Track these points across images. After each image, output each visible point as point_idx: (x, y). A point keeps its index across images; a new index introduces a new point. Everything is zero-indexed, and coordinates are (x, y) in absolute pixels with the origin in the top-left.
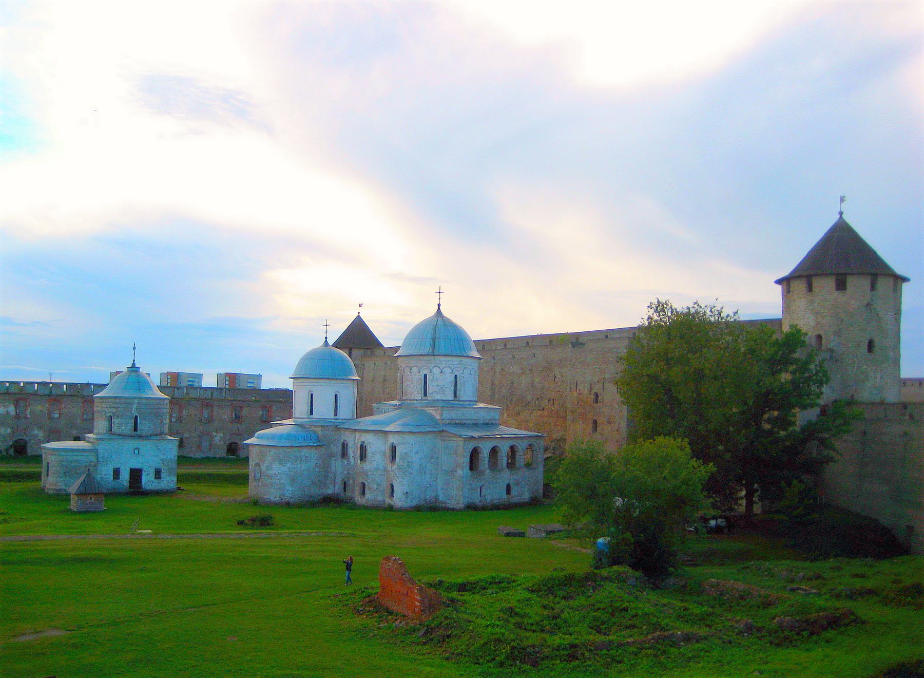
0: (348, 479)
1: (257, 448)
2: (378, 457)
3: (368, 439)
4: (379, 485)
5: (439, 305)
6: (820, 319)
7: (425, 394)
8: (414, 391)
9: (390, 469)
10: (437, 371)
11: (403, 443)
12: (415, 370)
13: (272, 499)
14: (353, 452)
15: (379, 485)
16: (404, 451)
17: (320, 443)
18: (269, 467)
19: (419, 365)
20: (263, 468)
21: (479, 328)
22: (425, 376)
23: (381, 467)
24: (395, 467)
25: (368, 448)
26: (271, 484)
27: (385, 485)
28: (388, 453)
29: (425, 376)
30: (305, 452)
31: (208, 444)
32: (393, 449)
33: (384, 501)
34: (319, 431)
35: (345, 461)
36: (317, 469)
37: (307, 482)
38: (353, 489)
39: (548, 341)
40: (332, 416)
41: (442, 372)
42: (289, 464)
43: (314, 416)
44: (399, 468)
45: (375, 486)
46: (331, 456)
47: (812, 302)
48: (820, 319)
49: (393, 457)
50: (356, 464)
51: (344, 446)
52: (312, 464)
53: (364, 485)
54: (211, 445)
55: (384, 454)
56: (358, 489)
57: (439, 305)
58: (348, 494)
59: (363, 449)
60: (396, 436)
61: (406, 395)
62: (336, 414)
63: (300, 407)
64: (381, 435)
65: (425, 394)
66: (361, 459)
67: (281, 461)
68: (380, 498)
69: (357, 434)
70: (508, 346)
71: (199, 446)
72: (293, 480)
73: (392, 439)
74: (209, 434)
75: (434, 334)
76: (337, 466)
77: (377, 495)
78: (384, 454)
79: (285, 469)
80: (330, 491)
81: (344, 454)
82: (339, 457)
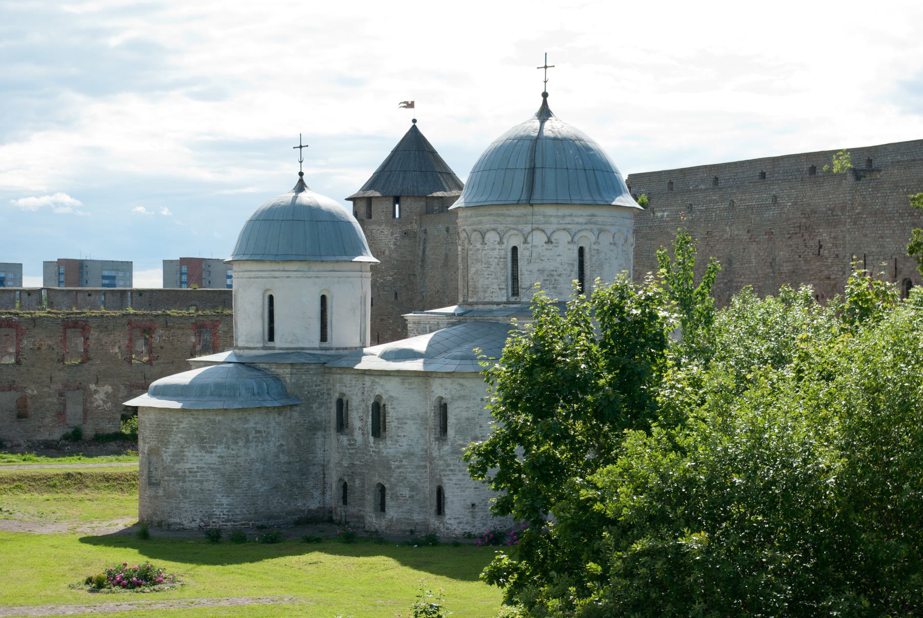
0: (352, 476)
1: (152, 416)
3: (389, 389)
4: (413, 488)
5: (545, 95)
7: (515, 293)
8: (490, 285)
9: (435, 454)
10: (539, 239)
11: (463, 397)
12: (492, 237)
13: (186, 524)
14: (359, 419)
15: (413, 488)
16: (465, 415)
17: (289, 400)
18: (179, 457)
19: (501, 228)
20: (167, 457)
21: (635, 146)
22: (515, 249)
23: (417, 450)
24: (447, 448)
25: (389, 408)
26: (183, 492)
27: (428, 489)
28: (433, 421)
29: (515, 249)
30: (255, 421)
31: (79, 409)
32: (443, 409)
33: (426, 524)
34: (285, 372)
35: (344, 439)
36: (283, 458)
37: (260, 486)
38: (363, 499)
39: (806, 167)
40: (313, 340)
41: (549, 241)
42: (220, 450)
43: (279, 342)
45: (406, 492)
46: (315, 427)
50: (366, 443)
51: (342, 405)
52: (272, 447)
53: (382, 489)
54: (85, 412)
55: (424, 420)
56: (371, 497)
57: (545, 95)
58: (352, 509)
59: (378, 411)
60: (448, 382)
61: (475, 292)
62: (324, 338)
63: (247, 323)
64: (416, 380)
65: (515, 293)
67: (203, 443)
68: (417, 517)
69: (367, 378)
70: (722, 183)
71: (61, 415)
72: (230, 482)
74: (81, 387)
75: (533, 159)
76: (332, 451)
77: (410, 511)
79: (211, 459)
80: (314, 505)
81: (342, 424)
82: (333, 431)
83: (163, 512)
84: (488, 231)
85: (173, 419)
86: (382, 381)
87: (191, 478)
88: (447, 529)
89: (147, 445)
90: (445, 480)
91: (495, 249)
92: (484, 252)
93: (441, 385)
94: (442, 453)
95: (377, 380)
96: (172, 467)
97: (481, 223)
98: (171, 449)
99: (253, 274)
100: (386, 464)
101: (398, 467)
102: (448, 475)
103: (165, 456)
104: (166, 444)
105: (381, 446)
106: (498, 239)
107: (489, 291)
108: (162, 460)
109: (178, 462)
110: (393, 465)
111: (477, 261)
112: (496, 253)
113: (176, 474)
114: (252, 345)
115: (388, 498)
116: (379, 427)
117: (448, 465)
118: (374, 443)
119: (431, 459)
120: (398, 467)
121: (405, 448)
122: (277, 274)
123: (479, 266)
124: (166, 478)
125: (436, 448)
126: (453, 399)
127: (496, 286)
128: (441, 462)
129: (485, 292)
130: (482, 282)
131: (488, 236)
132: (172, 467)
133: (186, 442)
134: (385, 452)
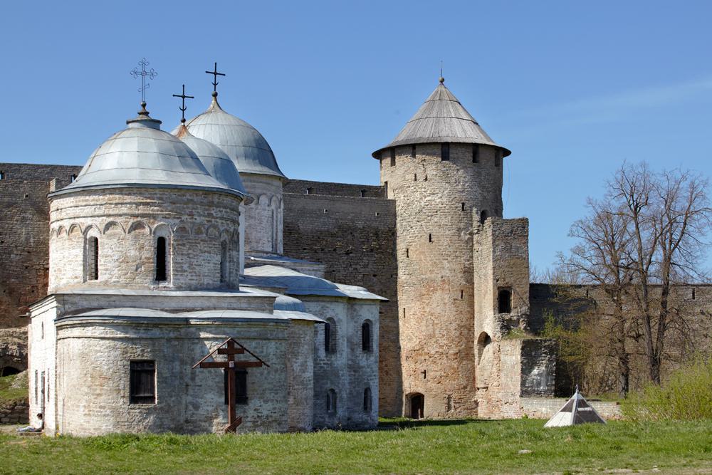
5: (215, 95)
6: (486, 194)
24: (372, 359)
28: (358, 339)
32: (366, 327)
48: (486, 194)
49: (366, 346)
66: (327, 349)
78: (349, 341)
83: (293, 418)
84: (260, 195)
85: (301, 332)
88: (373, 420)
91: (265, 210)
92: (258, 211)
93: (368, 310)
95: (328, 305)
96: (300, 376)
98: (301, 360)
102: (373, 379)
105: (333, 359)
108: (293, 370)
109: (304, 372)
118: (326, 356)
119: (354, 368)
120: (342, 376)
124: (296, 387)
125: (364, 359)
127: (266, 239)
128: (369, 370)
129: (258, 242)
131: (261, 198)
132: (300, 376)
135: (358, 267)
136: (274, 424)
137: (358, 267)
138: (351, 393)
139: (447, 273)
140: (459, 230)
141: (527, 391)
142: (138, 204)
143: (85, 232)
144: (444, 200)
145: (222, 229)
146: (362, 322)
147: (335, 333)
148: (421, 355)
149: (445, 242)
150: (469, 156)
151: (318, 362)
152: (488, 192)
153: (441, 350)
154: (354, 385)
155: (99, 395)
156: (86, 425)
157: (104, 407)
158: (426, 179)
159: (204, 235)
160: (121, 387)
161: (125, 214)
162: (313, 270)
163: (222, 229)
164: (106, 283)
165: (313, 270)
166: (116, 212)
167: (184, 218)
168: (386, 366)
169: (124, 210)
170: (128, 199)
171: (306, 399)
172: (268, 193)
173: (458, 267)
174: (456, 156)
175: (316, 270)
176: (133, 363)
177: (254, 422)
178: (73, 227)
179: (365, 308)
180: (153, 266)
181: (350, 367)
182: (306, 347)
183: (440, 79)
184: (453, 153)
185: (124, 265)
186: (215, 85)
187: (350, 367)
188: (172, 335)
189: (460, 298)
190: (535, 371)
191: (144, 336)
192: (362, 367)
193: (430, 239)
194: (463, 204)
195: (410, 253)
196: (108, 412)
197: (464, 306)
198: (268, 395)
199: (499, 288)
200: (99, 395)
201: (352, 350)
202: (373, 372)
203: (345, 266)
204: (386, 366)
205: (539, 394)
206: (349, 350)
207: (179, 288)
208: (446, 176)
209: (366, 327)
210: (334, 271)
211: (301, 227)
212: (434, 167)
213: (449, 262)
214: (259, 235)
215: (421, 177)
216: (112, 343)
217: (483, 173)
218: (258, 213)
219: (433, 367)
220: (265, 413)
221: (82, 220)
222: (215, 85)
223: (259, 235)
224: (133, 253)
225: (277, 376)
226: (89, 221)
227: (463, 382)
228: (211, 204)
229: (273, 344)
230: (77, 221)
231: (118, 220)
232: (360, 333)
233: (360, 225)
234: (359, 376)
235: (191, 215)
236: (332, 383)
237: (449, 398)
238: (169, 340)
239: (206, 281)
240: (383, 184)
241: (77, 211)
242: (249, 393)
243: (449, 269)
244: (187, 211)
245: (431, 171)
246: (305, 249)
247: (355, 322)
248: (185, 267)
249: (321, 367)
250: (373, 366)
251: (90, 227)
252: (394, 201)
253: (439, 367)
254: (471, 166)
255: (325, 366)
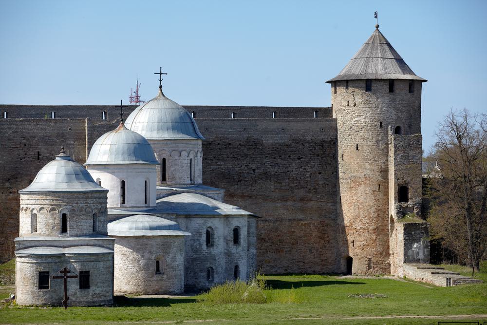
1: (158, 240)
2: (222, 240)
3: (216, 223)
5: (161, 87)
6: (399, 114)
12: (184, 154)
18: (174, 259)
22: (191, 160)
24: (240, 248)
28: (231, 237)
29: (191, 160)
32: (236, 232)
44: (243, 250)
47: (394, 100)
48: (399, 114)
56: (205, 274)
57: (161, 87)
59: (209, 235)
66: (207, 245)
73: (235, 223)
78: (225, 238)
83: (166, 286)
84: (182, 151)
85: (171, 241)
86: (212, 220)
87: (178, 269)
89: (154, 256)
90: (239, 262)
91: (185, 159)
92: (180, 161)
93: (237, 221)
94: (238, 251)
97: (178, 147)
98: (171, 255)
99: (140, 170)
100: (214, 258)
101: (218, 259)
103: (167, 259)
104: (168, 253)
106: (187, 155)
107: (182, 178)
109: (174, 262)
110: (217, 258)
111: (175, 165)
112: (186, 161)
113: (172, 268)
114: (139, 206)
115: (215, 273)
116: (209, 241)
117: (241, 256)
118: (207, 249)
119: (228, 254)
120: (218, 259)
121: (219, 251)
122: (150, 170)
123: (177, 167)
124: (168, 270)
126: (243, 227)
128: (237, 255)
130: (178, 175)
131: (182, 153)
133: (177, 252)
134: (213, 252)
135: (307, 167)
136: (102, 297)
137: (307, 167)
138: (226, 269)
139: (368, 172)
140: (377, 141)
141: (408, 260)
142: (53, 200)
143: (32, 211)
144: (367, 120)
145: (93, 208)
146: (233, 228)
147: (213, 235)
148: (351, 230)
149: (367, 150)
150: (386, 87)
151: (202, 252)
152: (402, 113)
153: (364, 227)
154: (228, 264)
155: (27, 286)
156: (22, 298)
157: (28, 291)
158: (355, 105)
159: (84, 212)
160: (35, 283)
161: (48, 204)
162: (216, 194)
163: (93, 208)
164: (40, 234)
165: (216, 194)
166: (44, 203)
167: (74, 205)
168: (328, 237)
169: (47, 202)
170: (49, 198)
171: (175, 276)
172: (188, 150)
173: (376, 168)
174: (376, 88)
175: (218, 194)
176: (40, 273)
177: (92, 296)
178: (27, 208)
179: (235, 219)
180: (60, 227)
181: (226, 254)
182: (175, 248)
183: (376, 25)
184: (374, 86)
185: (47, 226)
186: (161, 81)
187: (226, 254)
188: (57, 261)
189: (377, 190)
190: (415, 246)
191: (45, 262)
192: (234, 253)
193: (357, 148)
194: (381, 123)
195: (344, 157)
196: (30, 293)
197: (380, 195)
198: (99, 285)
199: (399, 185)
200: (27, 286)
201: (227, 244)
202: (241, 256)
203: (297, 167)
204: (328, 237)
205: (418, 261)
206: (225, 244)
207: (71, 236)
208: (368, 104)
209: (236, 232)
210: (288, 171)
211: (264, 142)
212: (360, 96)
213: (369, 165)
214: (181, 175)
215: (351, 103)
216: (31, 265)
217: (398, 100)
218: (181, 162)
219: (358, 238)
220: (98, 292)
221: (31, 206)
222: (161, 81)
223: (181, 175)
224: (51, 221)
225: (104, 277)
226: (33, 207)
227: (380, 249)
228: (87, 198)
229: (102, 263)
230: (29, 206)
231: (45, 206)
232: (232, 234)
233: (309, 138)
234: (231, 258)
235: (77, 203)
236: (210, 264)
237: (370, 260)
238: (56, 263)
239: (85, 232)
240: (331, 106)
241: (28, 202)
242: (90, 284)
243: (370, 170)
244: (75, 202)
245: (358, 100)
246: (267, 157)
247: (229, 228)
248: (75, 226)
249: (204, 255)
250: (241, 253)
251: (33, 209)
252: (336, 120)
253: (363, 239)
254: (388, 95)
255: (206, 254)
